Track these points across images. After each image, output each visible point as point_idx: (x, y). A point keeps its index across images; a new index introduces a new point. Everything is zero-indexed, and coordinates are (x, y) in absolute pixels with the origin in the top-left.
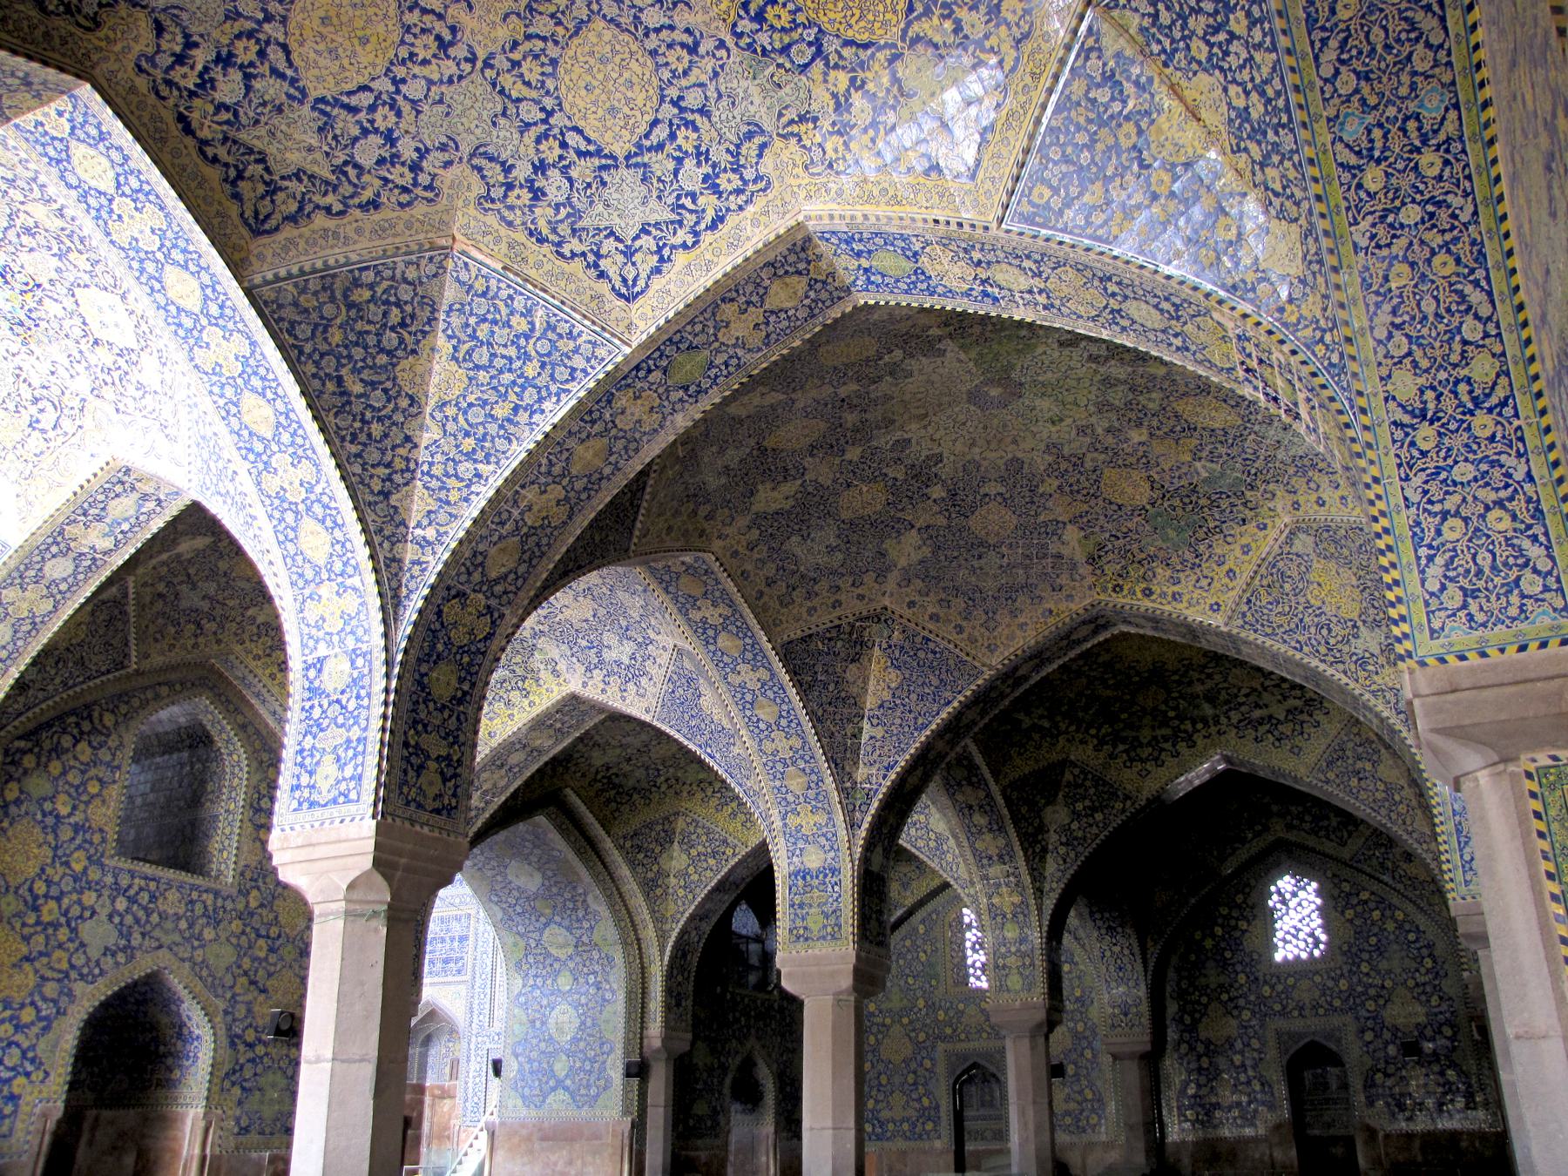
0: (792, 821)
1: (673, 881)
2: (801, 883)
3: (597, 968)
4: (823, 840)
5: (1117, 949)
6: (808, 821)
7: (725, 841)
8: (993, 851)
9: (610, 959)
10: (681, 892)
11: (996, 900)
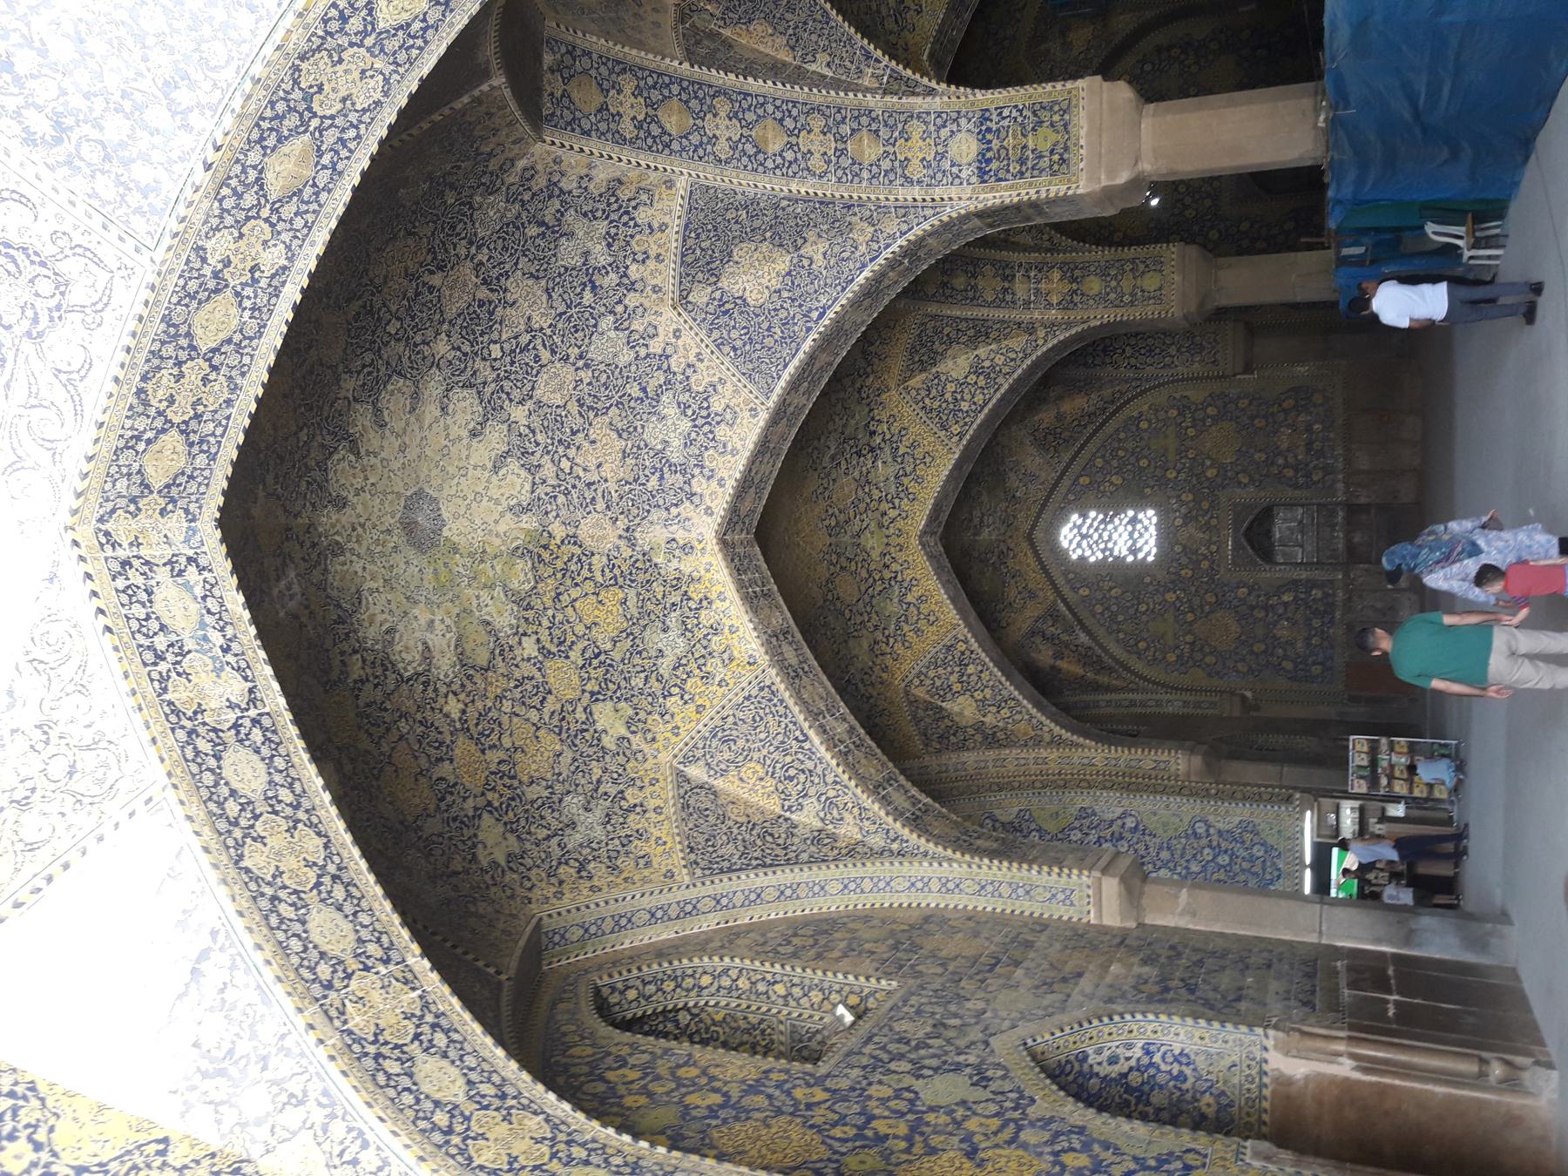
0: (916, 170)
1: (988, 719)
2: (994, 165)
3: (1093, 837)
4: (944, 132)
5: (1129, 351)
6: (917, 148)
7: (949, 648)
8: (999, 284)
9: (1084, 813)
10: (1005, 712)
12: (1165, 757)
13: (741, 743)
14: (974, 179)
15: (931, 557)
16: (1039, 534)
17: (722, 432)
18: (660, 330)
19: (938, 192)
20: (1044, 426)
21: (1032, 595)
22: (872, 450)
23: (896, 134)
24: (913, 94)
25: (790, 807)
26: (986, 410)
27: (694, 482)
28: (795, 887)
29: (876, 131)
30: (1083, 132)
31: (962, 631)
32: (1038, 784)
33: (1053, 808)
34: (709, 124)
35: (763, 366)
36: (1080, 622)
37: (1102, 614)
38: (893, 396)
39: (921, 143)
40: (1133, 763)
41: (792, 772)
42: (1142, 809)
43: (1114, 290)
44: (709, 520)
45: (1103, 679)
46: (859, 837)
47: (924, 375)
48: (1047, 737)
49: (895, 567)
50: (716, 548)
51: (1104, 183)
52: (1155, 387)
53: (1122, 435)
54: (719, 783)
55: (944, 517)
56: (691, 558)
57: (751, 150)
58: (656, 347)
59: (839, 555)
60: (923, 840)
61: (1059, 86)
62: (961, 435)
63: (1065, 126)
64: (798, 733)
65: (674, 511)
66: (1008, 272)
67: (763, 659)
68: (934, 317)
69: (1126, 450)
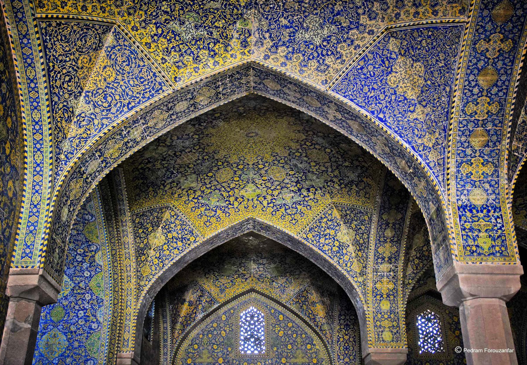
0: (465, 169)
1: (152, 253)
2: (468, 214)
3: (87, 306)
4: (487, 186)
5: (346, 337)
6: (478, 170)
7: (191, 232)
8: (387, 255)
10: (156, 261)
11: (377, 286)
12: (130, 345)
13: (127, 68)
14: (460, 203)
15: (241, 224)
16: (253, 295)
17: (314, 64)
18: (373, 22)
19: (452, 182)
20: (309, 296)
21: (222, 291)
22: (299, 190)
23: (486, 158)
24: (509, 169)
25: (88, 96)
26: (320, 252)
27: (284, 48)
28: (35, 89)
29: (487, 145)
30: (489, 263)
31: (201, 240)
32: (116, 276)
33: (102, 285)
34: (497, 37)
35: (352, 87)
36: (208, 315)
37: (212, 327)
38: (328, 200)
39: (481, 172)
40: (127, 328)
41: (109, 99)
42: (102, 332)
43: (383, 317)
44: (262, 57)
45: (178, 326)
46: (69, 136)
47: (339, 217)
48: (142, 283)
49: (236, 204)
50: (245, 62)
51: (460, 276)
52: (328, 351)
53: (304, 336)
54: (103, 53)
55: (263, 233)
56: (239, 46)
57: (481, 64)
58: (364, 19)
59: (242, 170)
60: (66, 173)
61: (516, 250)
62: (307, 239)
63: (493, 254)
64: (133, 104)
65: (267, 35)
66: (393, 260)
67: (179, 86)
68: (370, 219)
69: (296, 338)
